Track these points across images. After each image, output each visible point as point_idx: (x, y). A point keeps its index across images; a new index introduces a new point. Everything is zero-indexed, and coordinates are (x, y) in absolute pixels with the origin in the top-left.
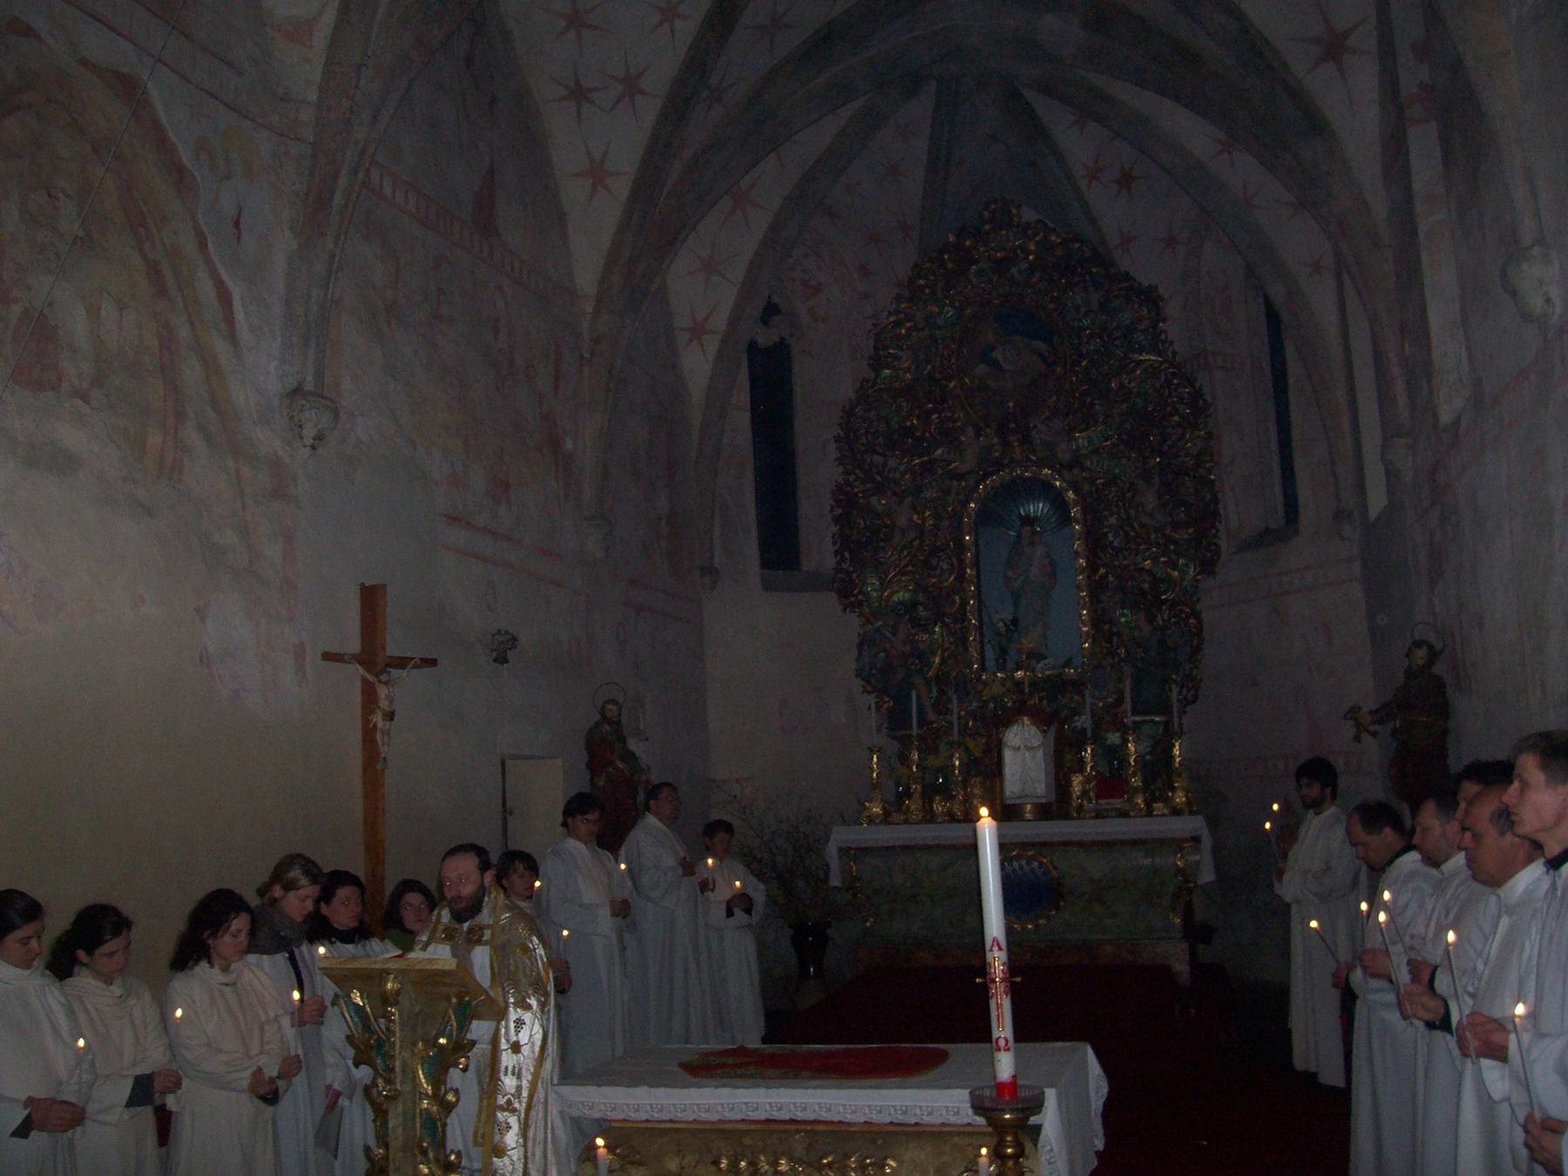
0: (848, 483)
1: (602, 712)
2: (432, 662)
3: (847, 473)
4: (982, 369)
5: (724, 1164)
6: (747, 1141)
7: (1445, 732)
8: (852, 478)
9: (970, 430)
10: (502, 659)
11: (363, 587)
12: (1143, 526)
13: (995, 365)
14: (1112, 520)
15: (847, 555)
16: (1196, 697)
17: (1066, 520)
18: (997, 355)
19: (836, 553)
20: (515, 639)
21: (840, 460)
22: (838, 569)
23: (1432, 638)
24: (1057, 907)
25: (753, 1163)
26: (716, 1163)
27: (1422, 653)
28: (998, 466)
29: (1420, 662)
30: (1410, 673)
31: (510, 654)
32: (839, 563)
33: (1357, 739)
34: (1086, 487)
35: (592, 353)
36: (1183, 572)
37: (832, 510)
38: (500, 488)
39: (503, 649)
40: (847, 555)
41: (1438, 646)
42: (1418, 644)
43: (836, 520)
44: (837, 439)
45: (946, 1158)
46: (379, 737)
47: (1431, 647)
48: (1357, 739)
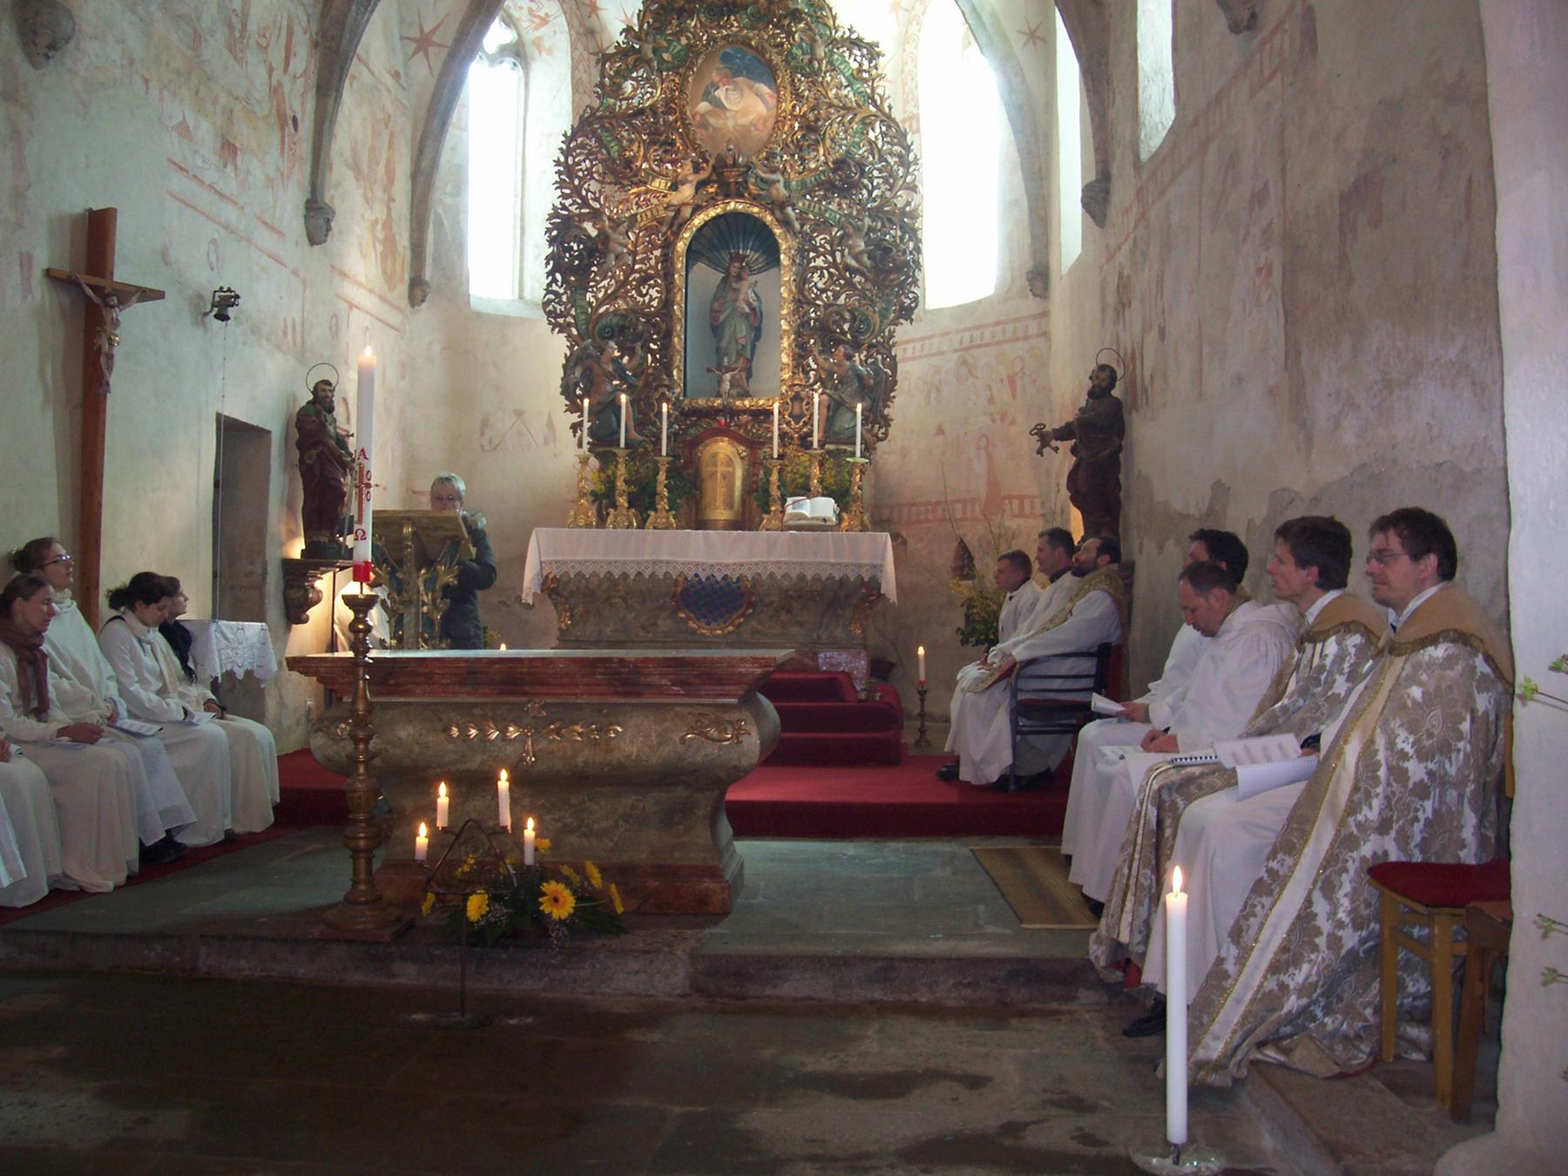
0: (564, 207)
1: (315, 392)
2: (160, 295)
3: (564, 196)
4: (704, 106)
5: (455, 731)
6: (477, 711)
7: (1120, 449)
8: (568, 202)
9: (689, 166)
10: (222, 317)
11: (90, 211)
12: (848, 268)
13: (717, 104)
14: (820, 262)
15: (558, 276)
16: (886, 434)
17: (773, 259)
18: (720, 93)
19: (549, 274)
20: (237, 297)
21: (561, 185)
22: (548, 292)
23: (1114, 365)
24: (747, 617)
25: (483, 732)
26: (447, 730)
27: (1104, 375)
28: (712, 201)
29: (1104, 384)
30: (1091, 394)
31: (231, 311)
32: (549, 285)
33: (1040, 452)
34: (797, 226)
35: (324, 36)
36: (883, 317)
37: (548, 231)
38: (228, 149)
39: (224, 305)
40: (558, 276)
41: (1120, 372)
42: (1102, 368)
43: (551, 241)
44: (558, 163)
45: (667, 724)
46: (103, 359)
47: (1113, 372)
48: (1040, 452)
